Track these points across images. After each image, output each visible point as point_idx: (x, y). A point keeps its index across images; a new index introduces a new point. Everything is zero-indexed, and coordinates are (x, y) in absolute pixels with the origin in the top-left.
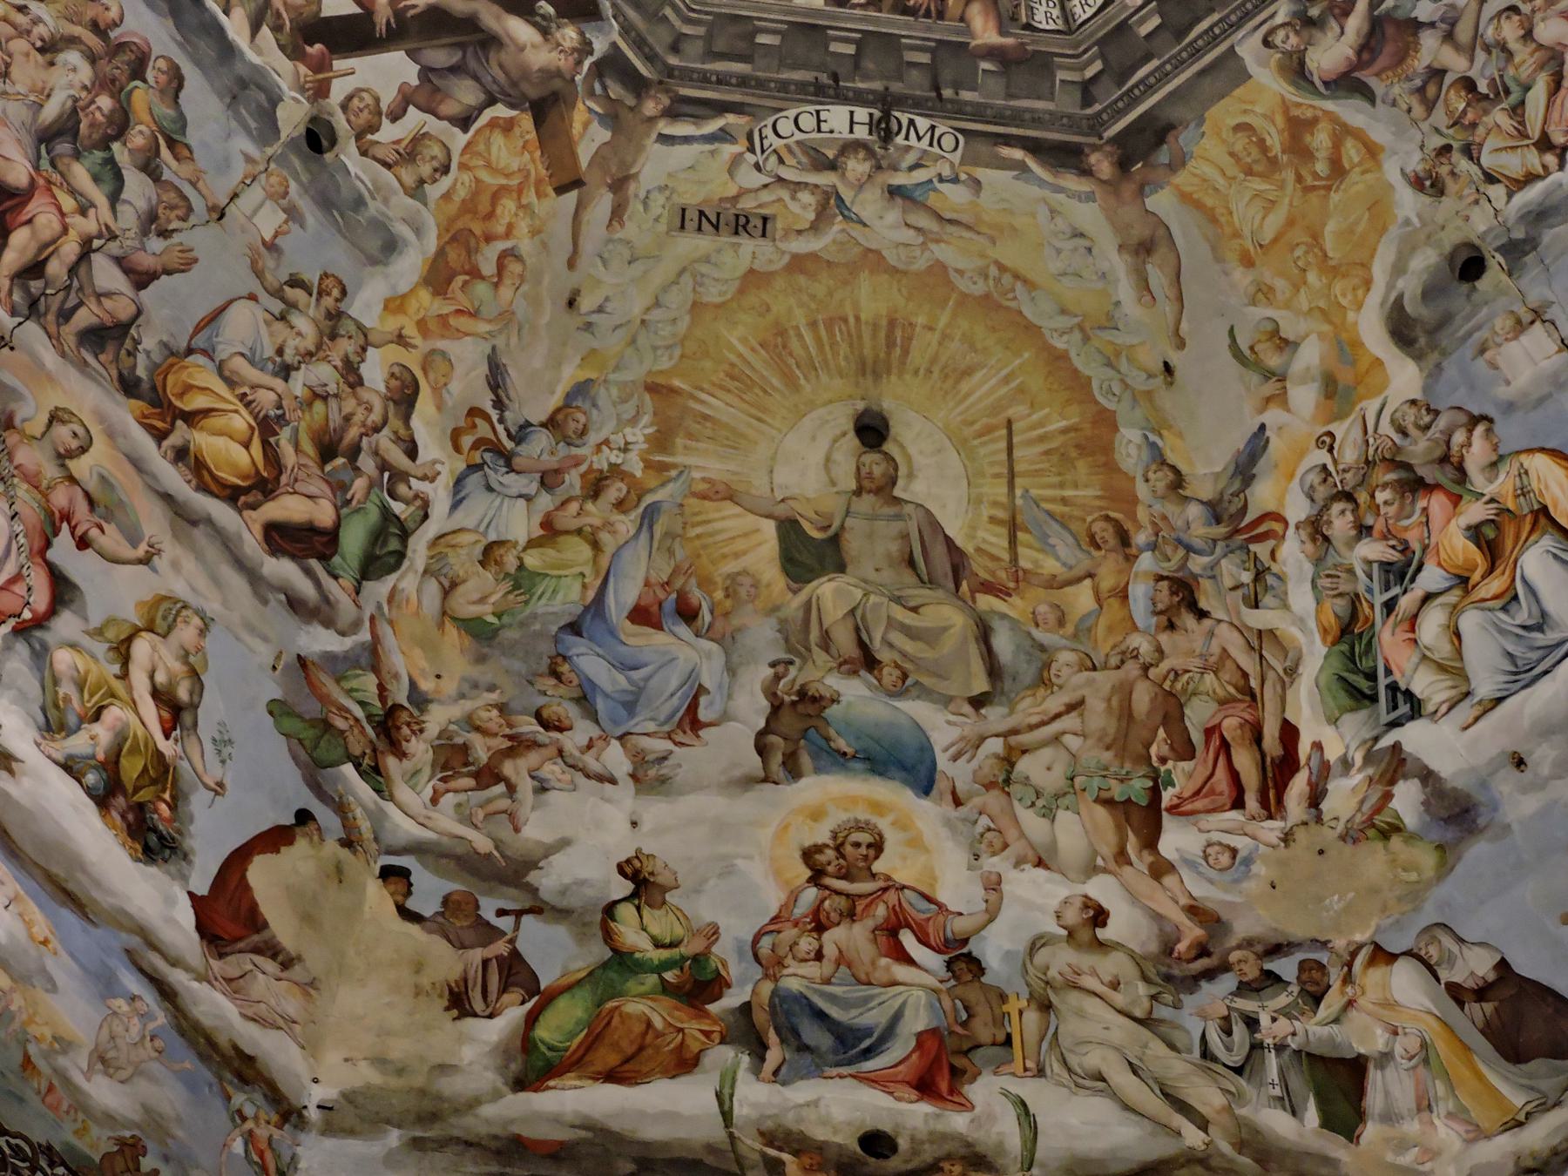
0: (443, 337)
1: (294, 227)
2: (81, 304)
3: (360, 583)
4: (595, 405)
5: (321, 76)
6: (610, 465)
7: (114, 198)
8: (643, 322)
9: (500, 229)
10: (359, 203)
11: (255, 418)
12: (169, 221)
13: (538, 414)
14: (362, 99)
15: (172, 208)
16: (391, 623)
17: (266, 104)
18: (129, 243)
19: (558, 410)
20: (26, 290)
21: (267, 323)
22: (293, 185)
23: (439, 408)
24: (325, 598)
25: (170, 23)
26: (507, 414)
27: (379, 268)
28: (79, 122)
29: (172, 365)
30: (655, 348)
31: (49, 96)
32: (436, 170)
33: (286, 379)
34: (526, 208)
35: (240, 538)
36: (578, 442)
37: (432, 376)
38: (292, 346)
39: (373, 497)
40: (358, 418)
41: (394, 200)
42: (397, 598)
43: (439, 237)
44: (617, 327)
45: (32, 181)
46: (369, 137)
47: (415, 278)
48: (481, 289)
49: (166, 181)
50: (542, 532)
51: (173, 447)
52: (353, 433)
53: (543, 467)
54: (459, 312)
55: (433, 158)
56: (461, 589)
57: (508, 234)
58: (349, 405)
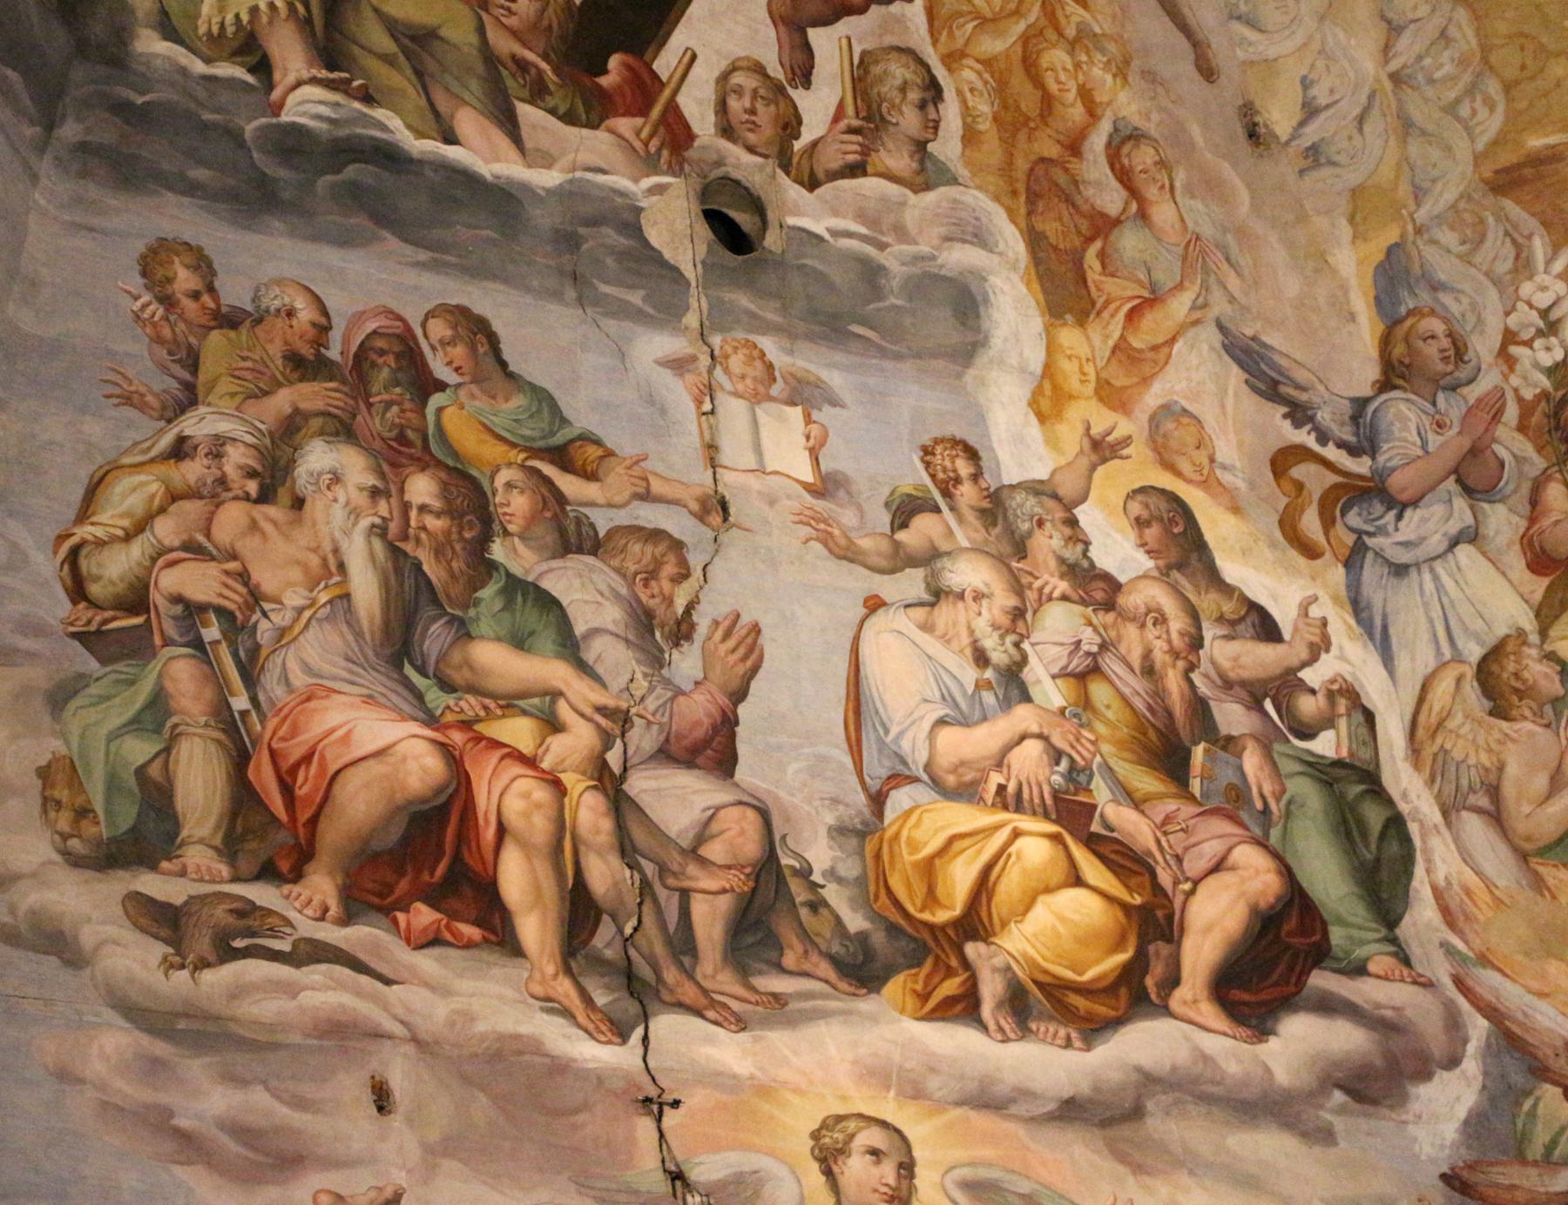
0: (1146, 381)
1: (825, 415)
2: (685, 894)
3: (1394, 941)
4: (1436, 287)
5: (656, 112)
6: (1550, 372)
7: (570, 647)
8: (1395, 78)
9: (1077, 113)
10: (871, 273)
11: (1046, 816)
12: (669, 601)
13: (1362, 373)
14: (739, 91)
15: (651, 575)
16: (1484, 960)
17: (623, 241)
18: (651, 704)
19: (1386, 342)
20: (599, 964)
21: (927, 627)
22: (769, 345)
23: (1236, 510)
24: (1383, 1025)
25: (392, 242)
26: (1324, 416)
27: (982, 359)
28: (418, 567)
29: (878, 856)
30: (1451, 109)
31: (342, 567)
32: (922, 106)
33: (1026, 698)
34: (1082, 41)
35: (1206, 1059)
36: (1462, 374)
37: (1185, 466)
38: (984, 622)
39: (1287, 766)
40: (1159, 656)
41: (910, 218)
42: (1455, 898)
43: (1013, 221)
44: (1361, 120)
45: (445, 749)
46: (798, 145)
47: (1037, 323)
48: (1130, 242)
49: (613, 532)
50: (1546, 581)
51: (999, 1005)
52: (1173, 681)
53: (1451, 457)
54: (1132, 316)
55: (903, 89)
56: (1509, 790)
57: (1093, 113)
58: (1132, 641)
